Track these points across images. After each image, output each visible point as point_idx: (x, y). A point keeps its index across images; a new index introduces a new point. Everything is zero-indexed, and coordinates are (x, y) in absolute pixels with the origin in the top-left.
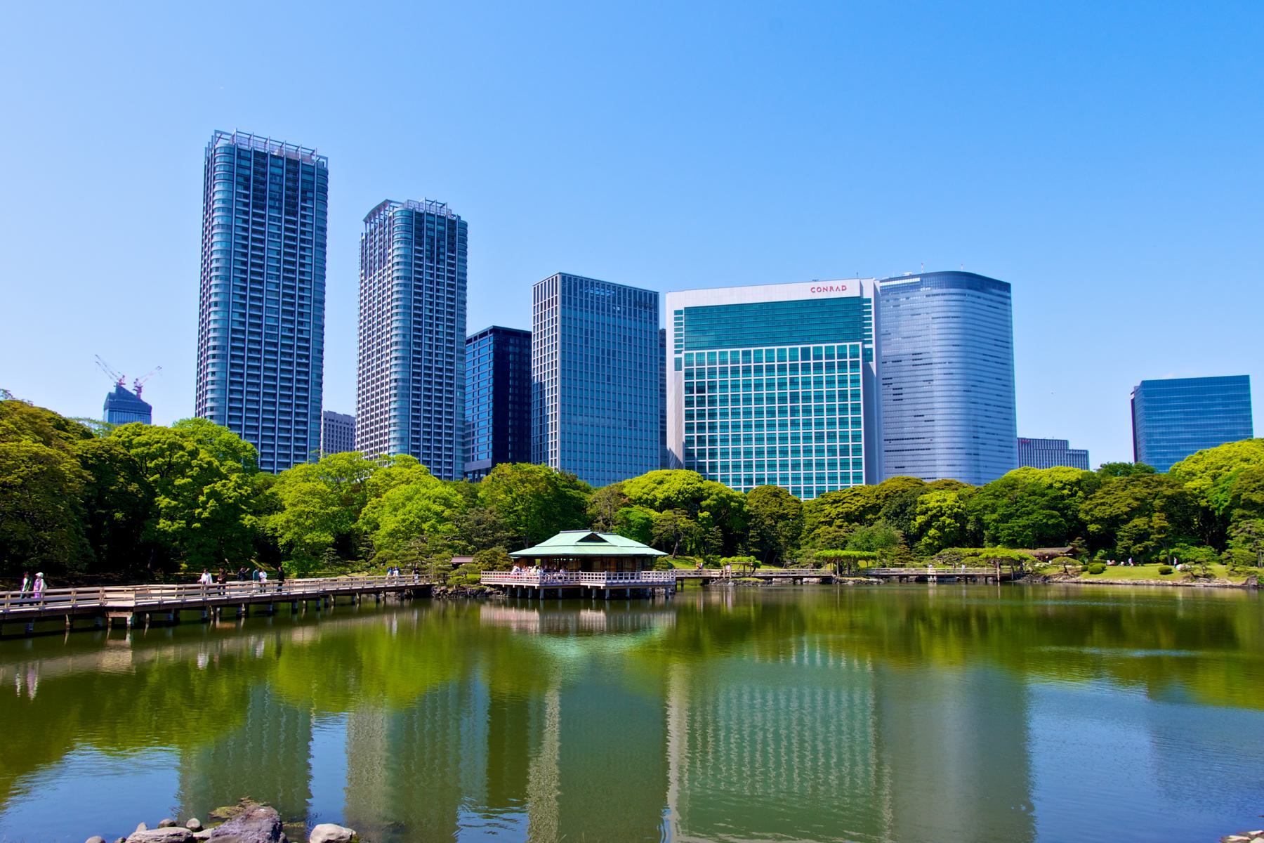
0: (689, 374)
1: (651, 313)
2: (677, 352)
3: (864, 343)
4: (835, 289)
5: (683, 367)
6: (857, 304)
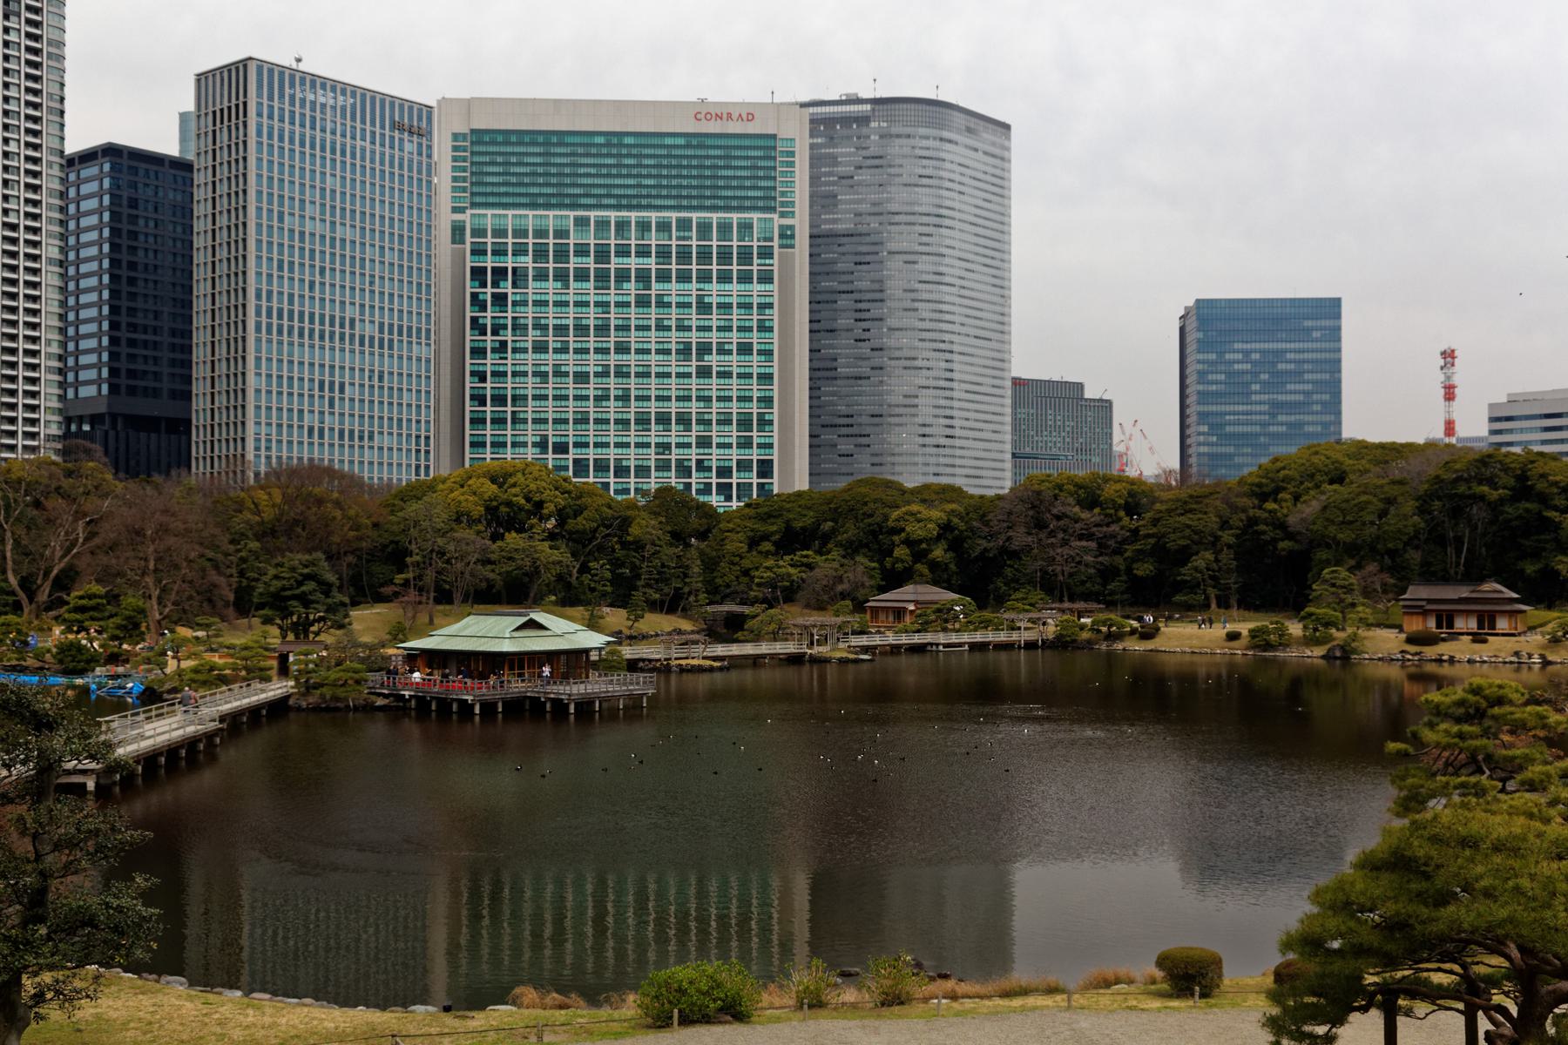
0: (478, 251)
1: (420, 145)
2: (455, 210)
3: (783, 215)
4: (735, 116)
5: (468, 239)
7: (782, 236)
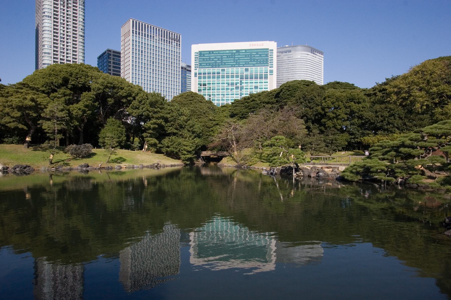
1: (177, 44)
3: (270, 67)
7: (270, 72)
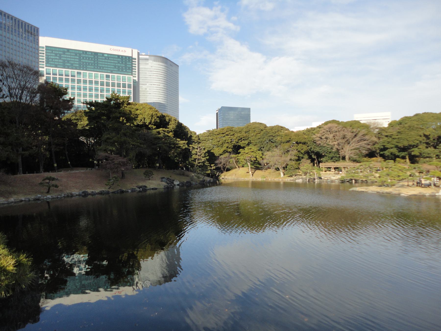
3: (133, 77)
4: (121, 51)
6: (130, 59)
